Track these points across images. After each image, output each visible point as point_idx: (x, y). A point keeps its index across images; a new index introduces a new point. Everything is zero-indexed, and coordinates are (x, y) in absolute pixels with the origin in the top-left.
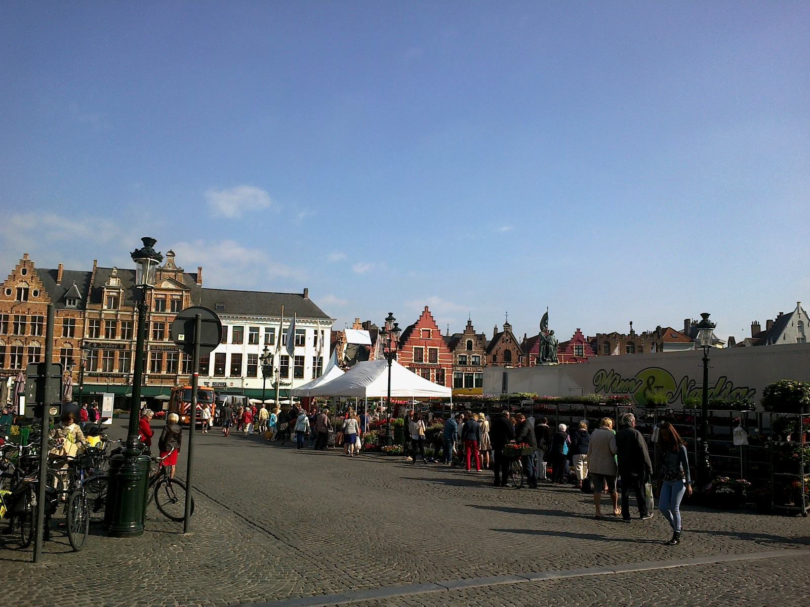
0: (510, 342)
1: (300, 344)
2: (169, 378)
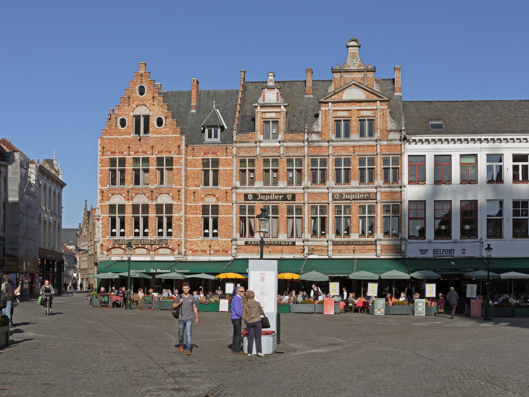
2: (365, 244)
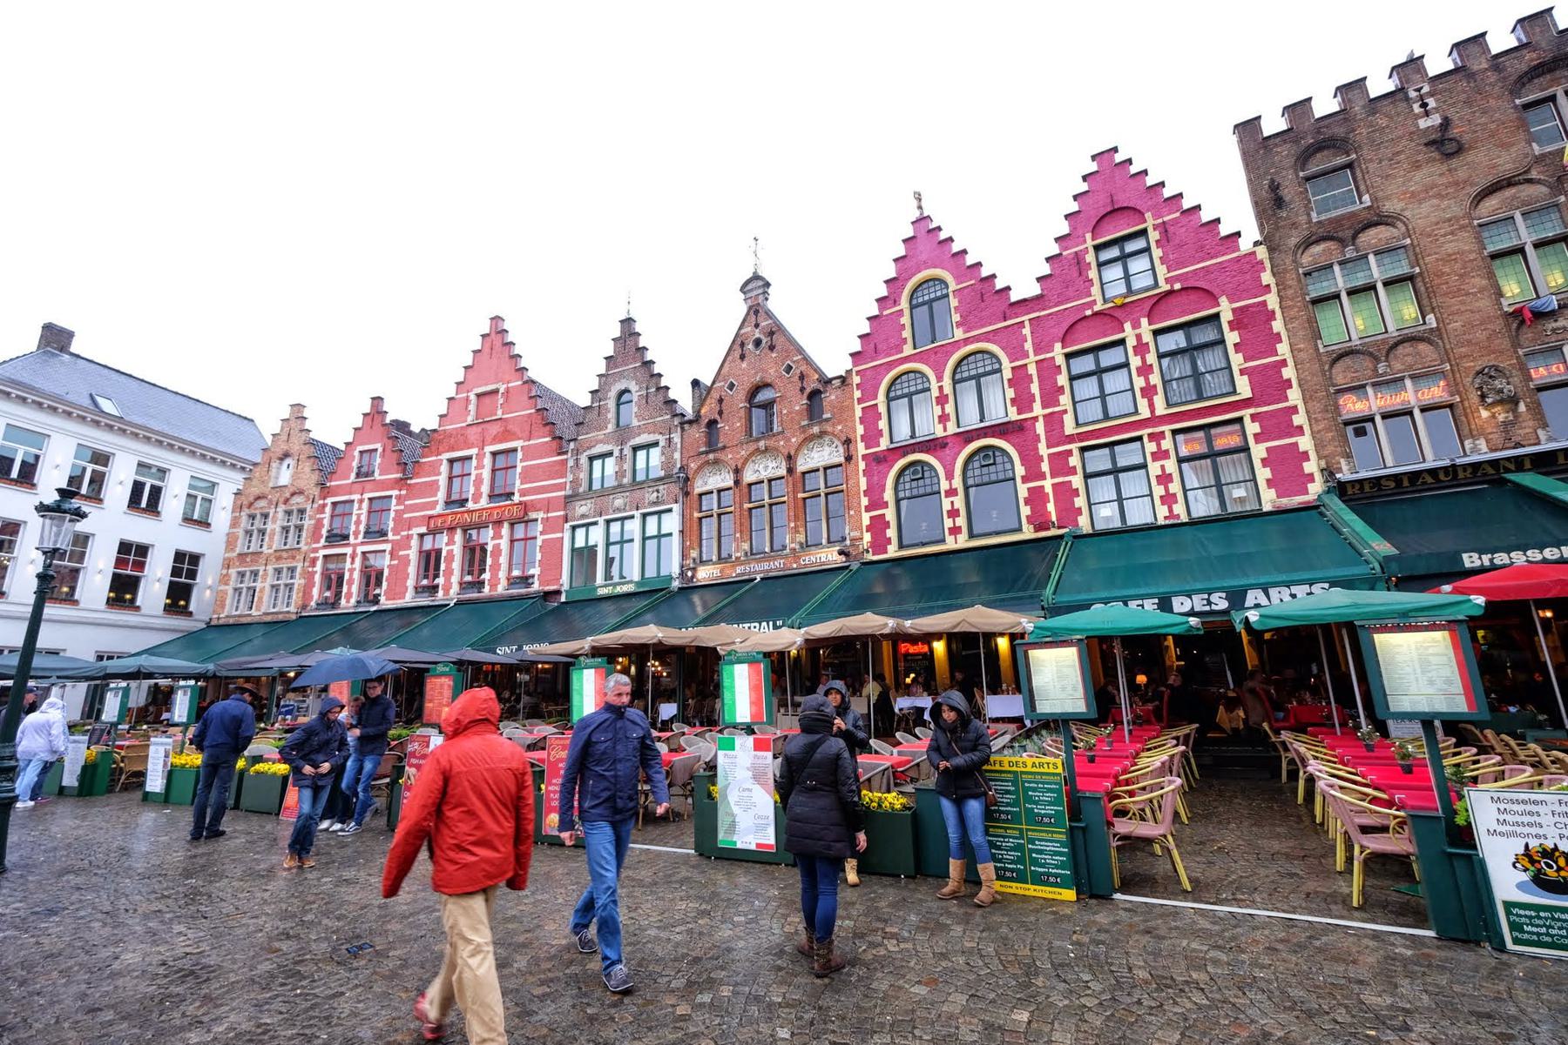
0: (772, 348)
1: (144, 505)
